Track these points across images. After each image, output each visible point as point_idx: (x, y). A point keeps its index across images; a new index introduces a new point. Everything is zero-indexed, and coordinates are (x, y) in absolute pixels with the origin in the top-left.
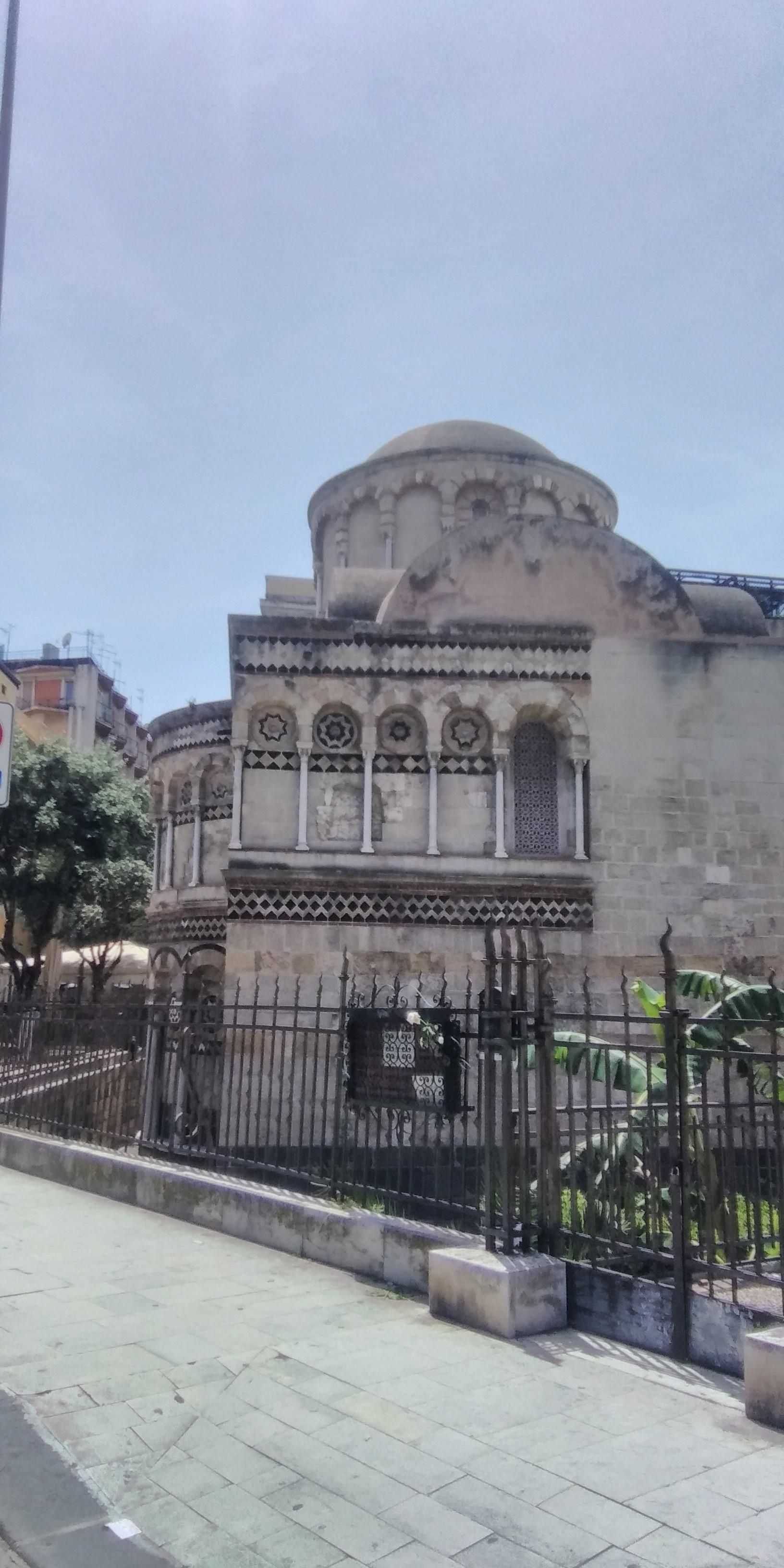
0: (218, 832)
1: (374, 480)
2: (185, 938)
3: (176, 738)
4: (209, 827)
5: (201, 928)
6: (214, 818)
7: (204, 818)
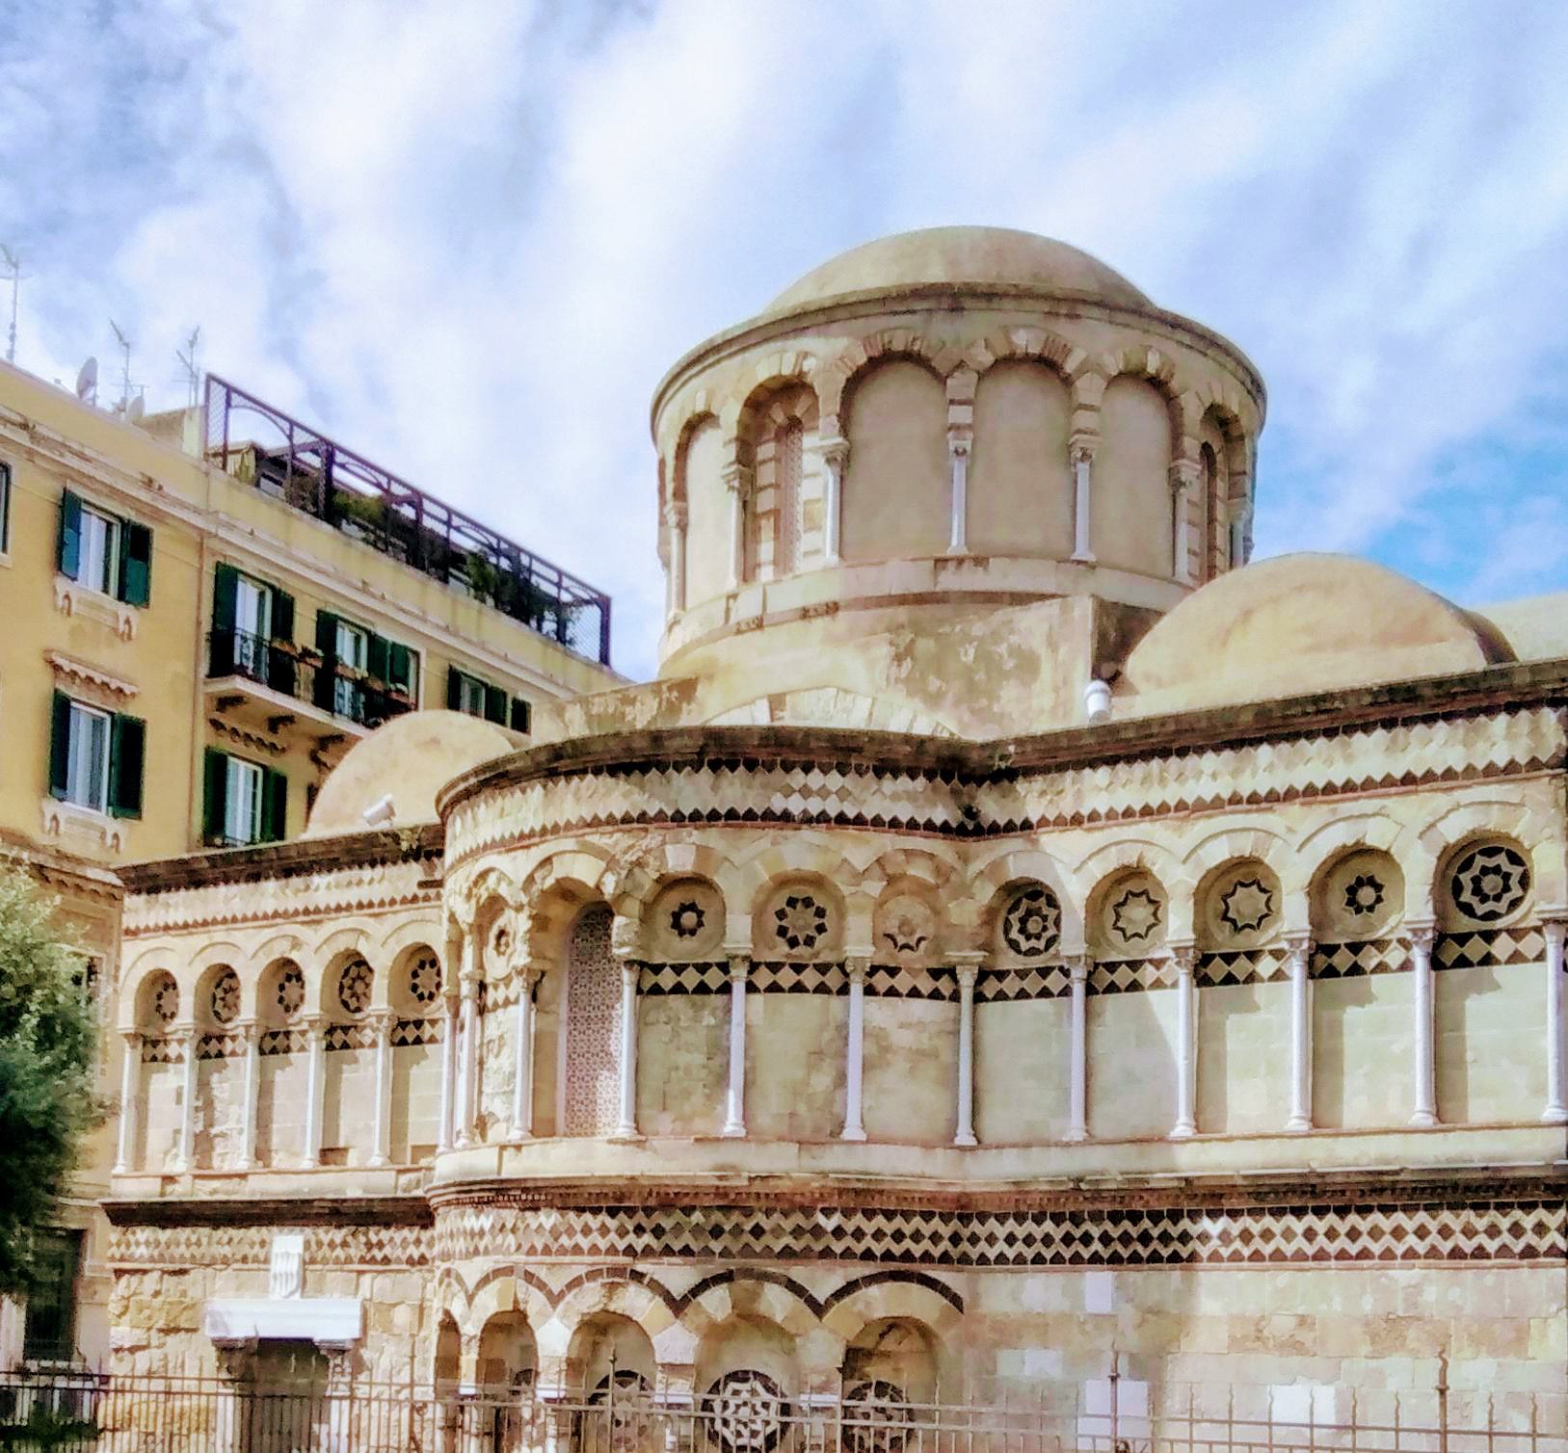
0: (902, 1026)
1: (1064, 330)
2: (827, 1253)
3: (788, 792)
4: (881, 1012)
5: (879, 1235)
6: (892, 992)
7: (870, 991)
